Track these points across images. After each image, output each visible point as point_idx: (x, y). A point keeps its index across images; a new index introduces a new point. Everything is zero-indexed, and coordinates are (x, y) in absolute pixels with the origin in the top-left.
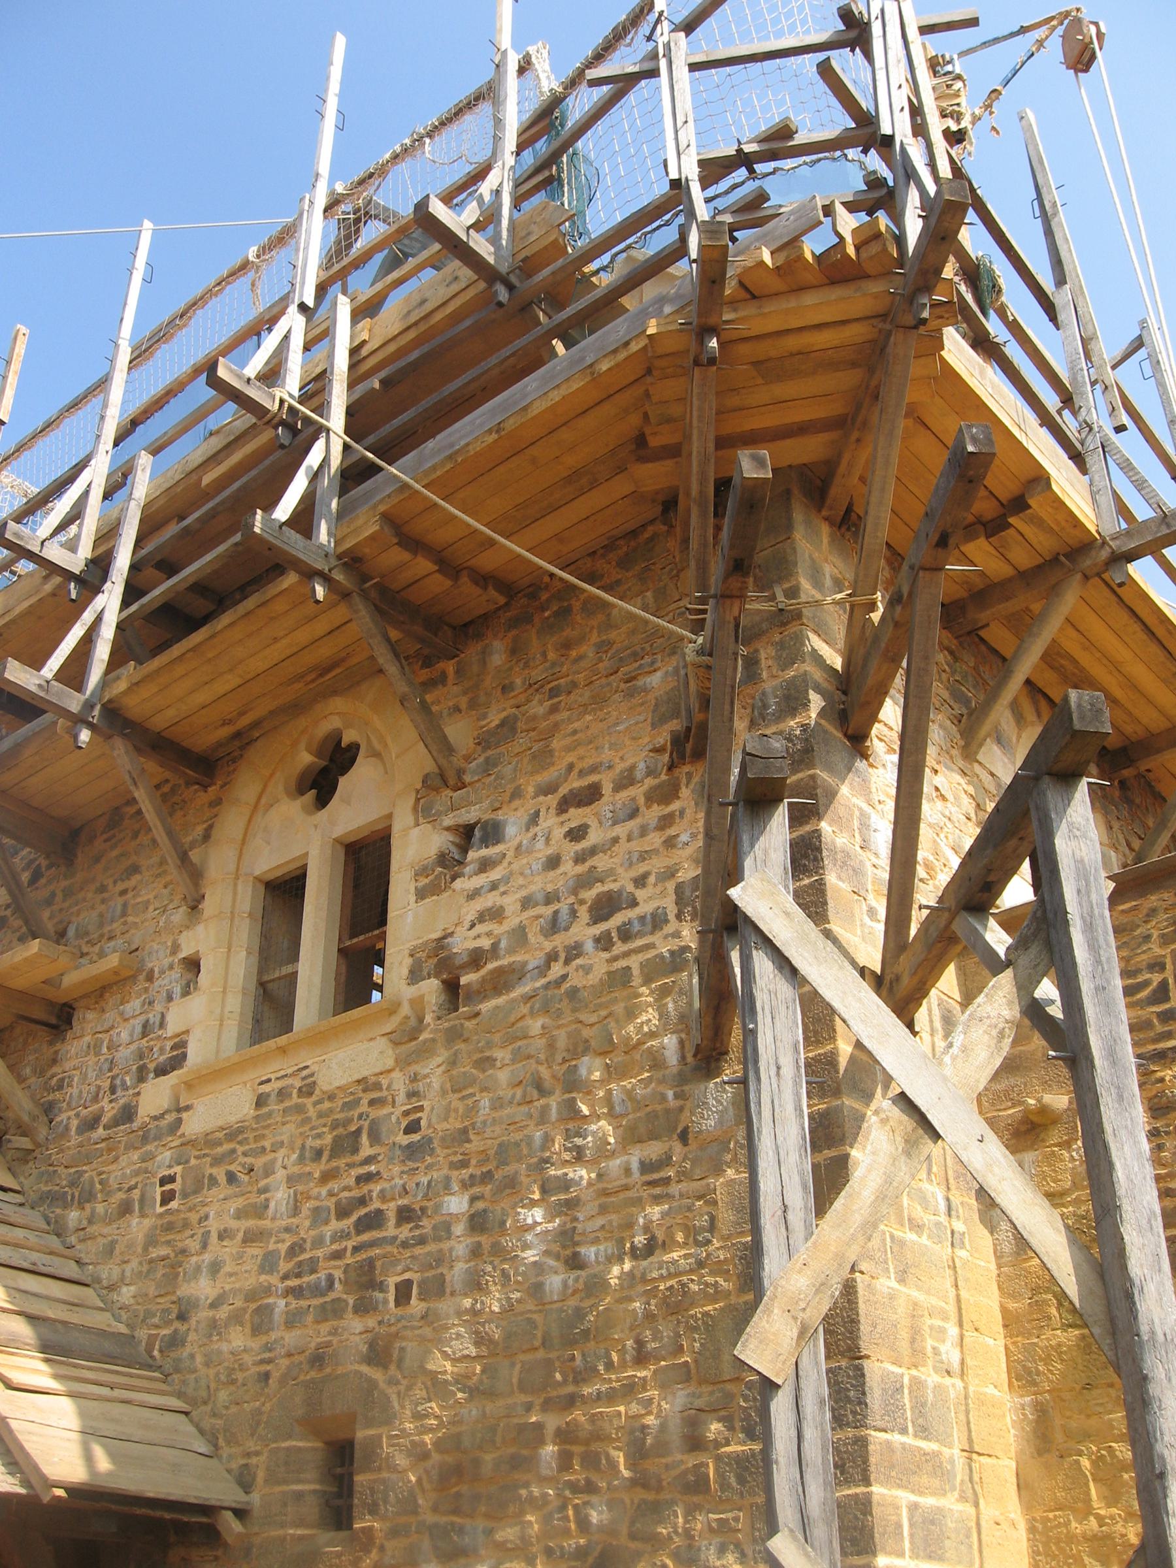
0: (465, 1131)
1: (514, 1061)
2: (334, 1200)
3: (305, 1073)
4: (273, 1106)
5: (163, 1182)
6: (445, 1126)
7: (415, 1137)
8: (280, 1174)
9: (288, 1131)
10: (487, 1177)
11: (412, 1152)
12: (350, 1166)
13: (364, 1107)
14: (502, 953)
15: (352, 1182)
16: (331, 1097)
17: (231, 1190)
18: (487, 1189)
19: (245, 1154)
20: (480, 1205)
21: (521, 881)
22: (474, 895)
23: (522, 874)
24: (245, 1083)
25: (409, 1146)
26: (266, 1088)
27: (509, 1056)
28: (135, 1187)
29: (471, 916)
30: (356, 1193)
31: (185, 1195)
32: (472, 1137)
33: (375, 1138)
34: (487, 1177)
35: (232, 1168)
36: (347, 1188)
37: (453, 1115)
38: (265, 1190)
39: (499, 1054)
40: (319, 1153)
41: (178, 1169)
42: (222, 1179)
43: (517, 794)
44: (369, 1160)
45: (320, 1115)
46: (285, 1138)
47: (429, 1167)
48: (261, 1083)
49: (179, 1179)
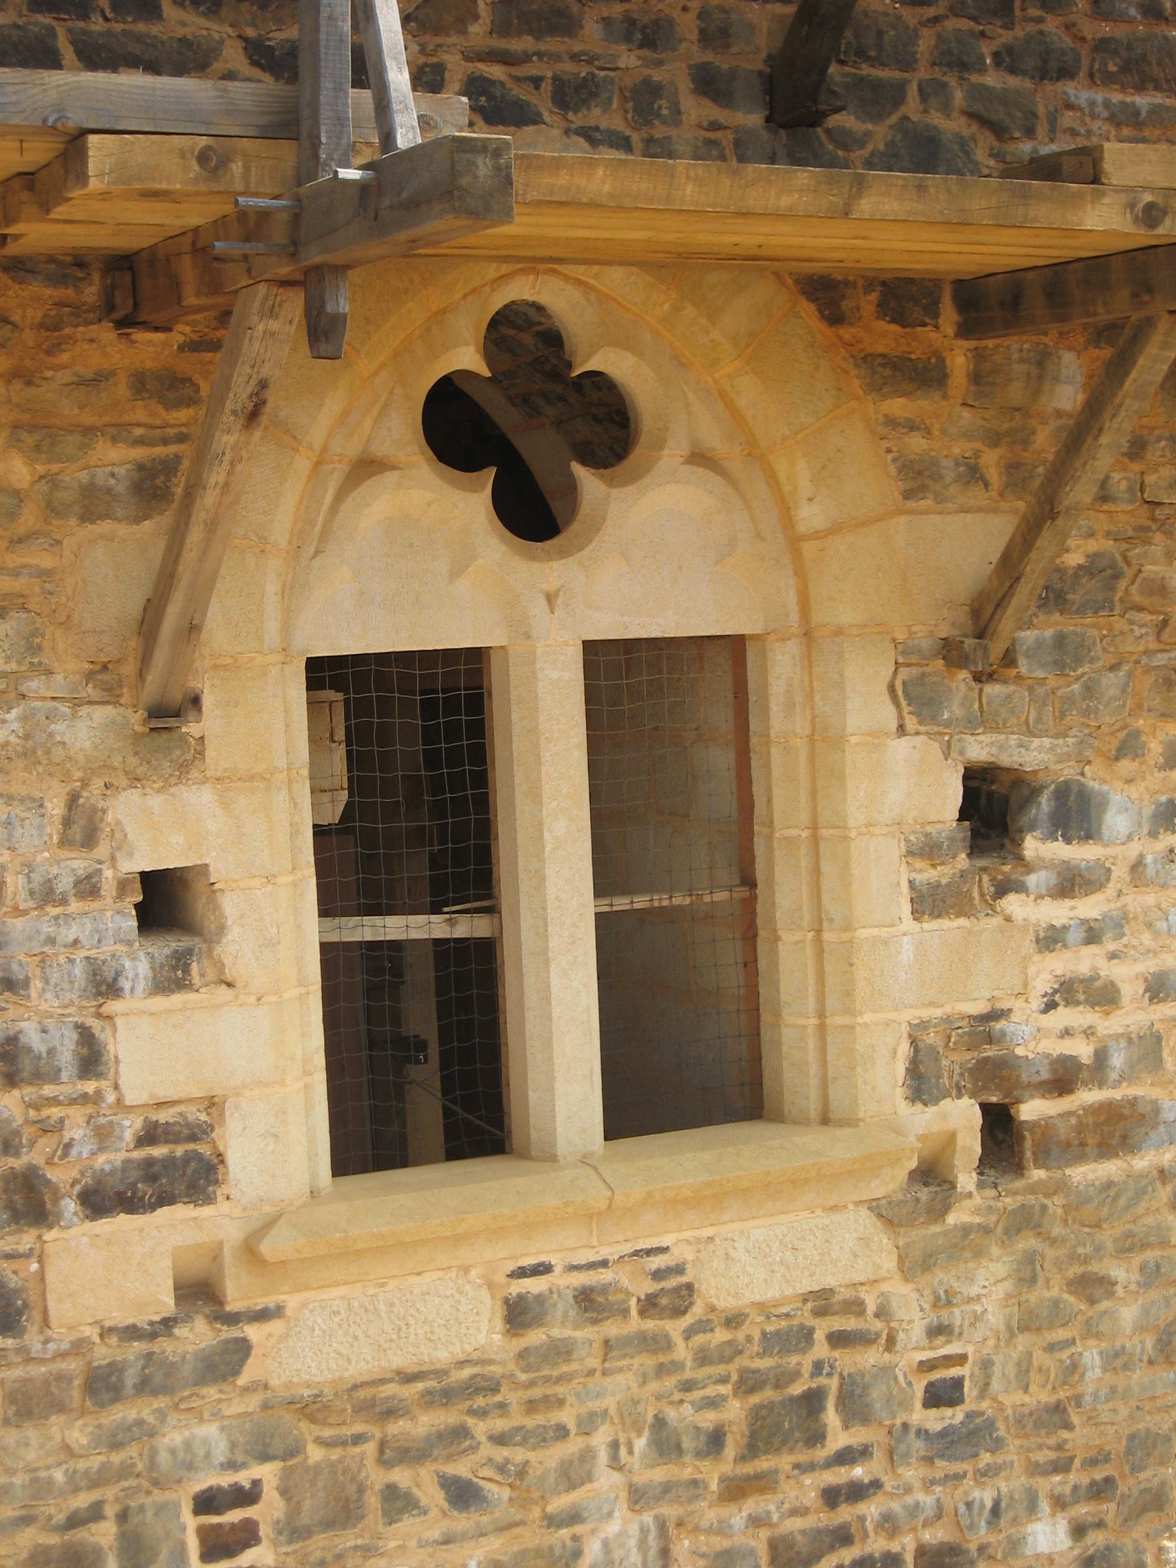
0: (1058, 1409)
1: (1146, 1285)
2: (764, 1533)
3: (656, 1262)
4: (561, 1327)
5: (206, 1503)
6: (1019, 1397)
7: (954, 1416)
8: (606, 1481)
9: (621, 1385)
10: (1100, 1490)
11: (947, 1444)
12: (811, 1467)
13: (821, 1349)
14: (1114, 1076)
15: (811, 1497)
16: (733, 1321)
17: (462, 1522)
18: (1109, 1509)
19: (500, 1440)
20: (1096, 1539)
21: (1147, 939)
22: (1051, 939)
23: (1149, 925)
24: (466, 1270)
25: (944, 1433)
26: (534, 1286)
27: (1135, 1277)
28: (95, 1513)
29: (1042, 984)
30: (824, 1519)
31: (293, 1531)
32: (1075, 1419)
33: (854, 1407)
34: (1100, 1490)
35: (461, 1469)
36: (797, 1512)
37: (1034, 1377)
38: (574, 1517)
39: (1121, 1273)
40: (715, 1440)
41: (267, 1473)
42: (432, 1495)
43: (1129, 747)
44: (845, 1457)
45: (703, 1358)
46: (610, 1403)
47: (984, 1474)
48: (521, 1273)
49: (270, 1493)
